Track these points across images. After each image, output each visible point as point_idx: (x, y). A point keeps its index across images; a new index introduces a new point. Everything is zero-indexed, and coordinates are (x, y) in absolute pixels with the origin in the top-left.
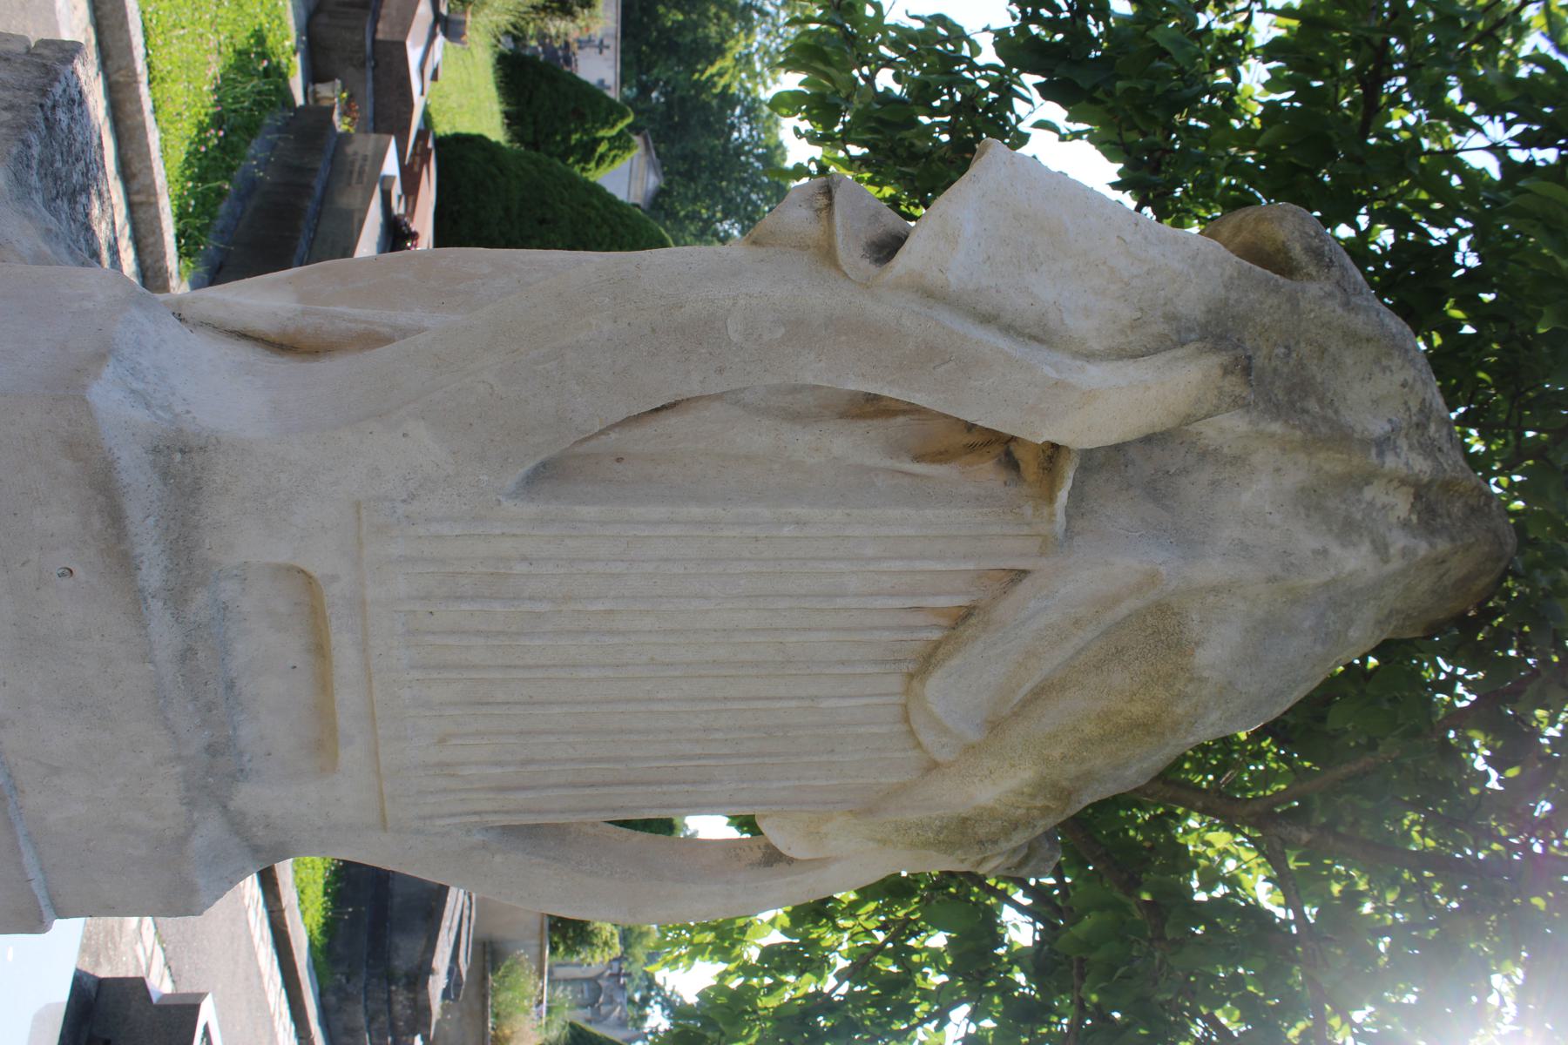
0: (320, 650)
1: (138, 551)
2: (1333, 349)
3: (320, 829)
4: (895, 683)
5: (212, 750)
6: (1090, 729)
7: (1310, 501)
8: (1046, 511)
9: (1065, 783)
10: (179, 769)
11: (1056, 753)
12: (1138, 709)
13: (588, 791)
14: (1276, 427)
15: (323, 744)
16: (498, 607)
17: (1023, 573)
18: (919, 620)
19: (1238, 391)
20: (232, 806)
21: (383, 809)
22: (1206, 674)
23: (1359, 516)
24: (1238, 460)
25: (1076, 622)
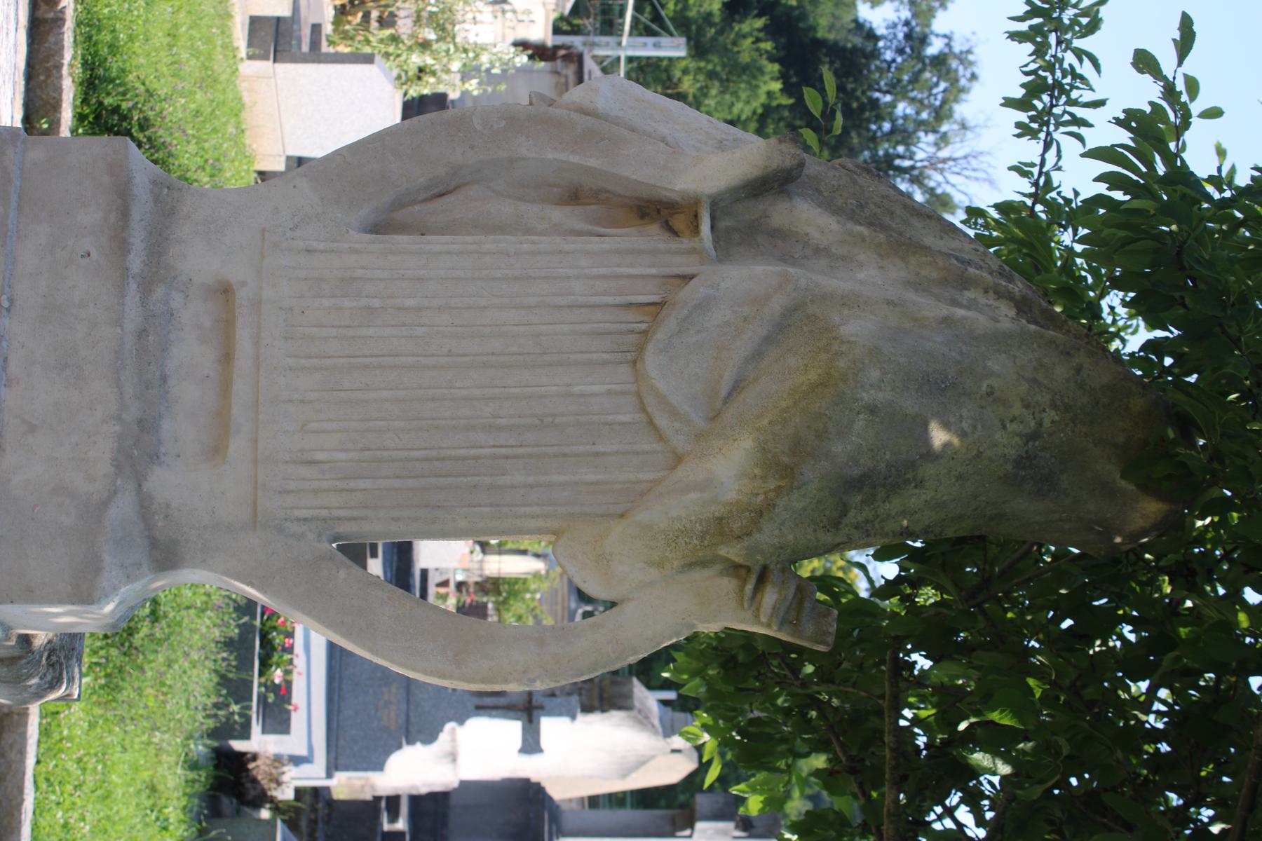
0: (227, 358)
1: (132, 240)
2: (898, 212)
3: (205, 527)
4: (624, 372)
5: (140, 422)
6: (784, 404)
7: (919, 285)
8: (696, 239)
10: (117, 428)
11: (765, 422)
12: (813, 376)
13: (411, 482)
14: (859, 228)
15: (216, 451)
16: (346, 303)
17: (692, 277)
18: (631, 316)
19: (793, 151)
20: (147, 486)
21: (255, 503)
22: (852, 339)
23: (965, 302)
24: (844, 258)
25: (745, 319)
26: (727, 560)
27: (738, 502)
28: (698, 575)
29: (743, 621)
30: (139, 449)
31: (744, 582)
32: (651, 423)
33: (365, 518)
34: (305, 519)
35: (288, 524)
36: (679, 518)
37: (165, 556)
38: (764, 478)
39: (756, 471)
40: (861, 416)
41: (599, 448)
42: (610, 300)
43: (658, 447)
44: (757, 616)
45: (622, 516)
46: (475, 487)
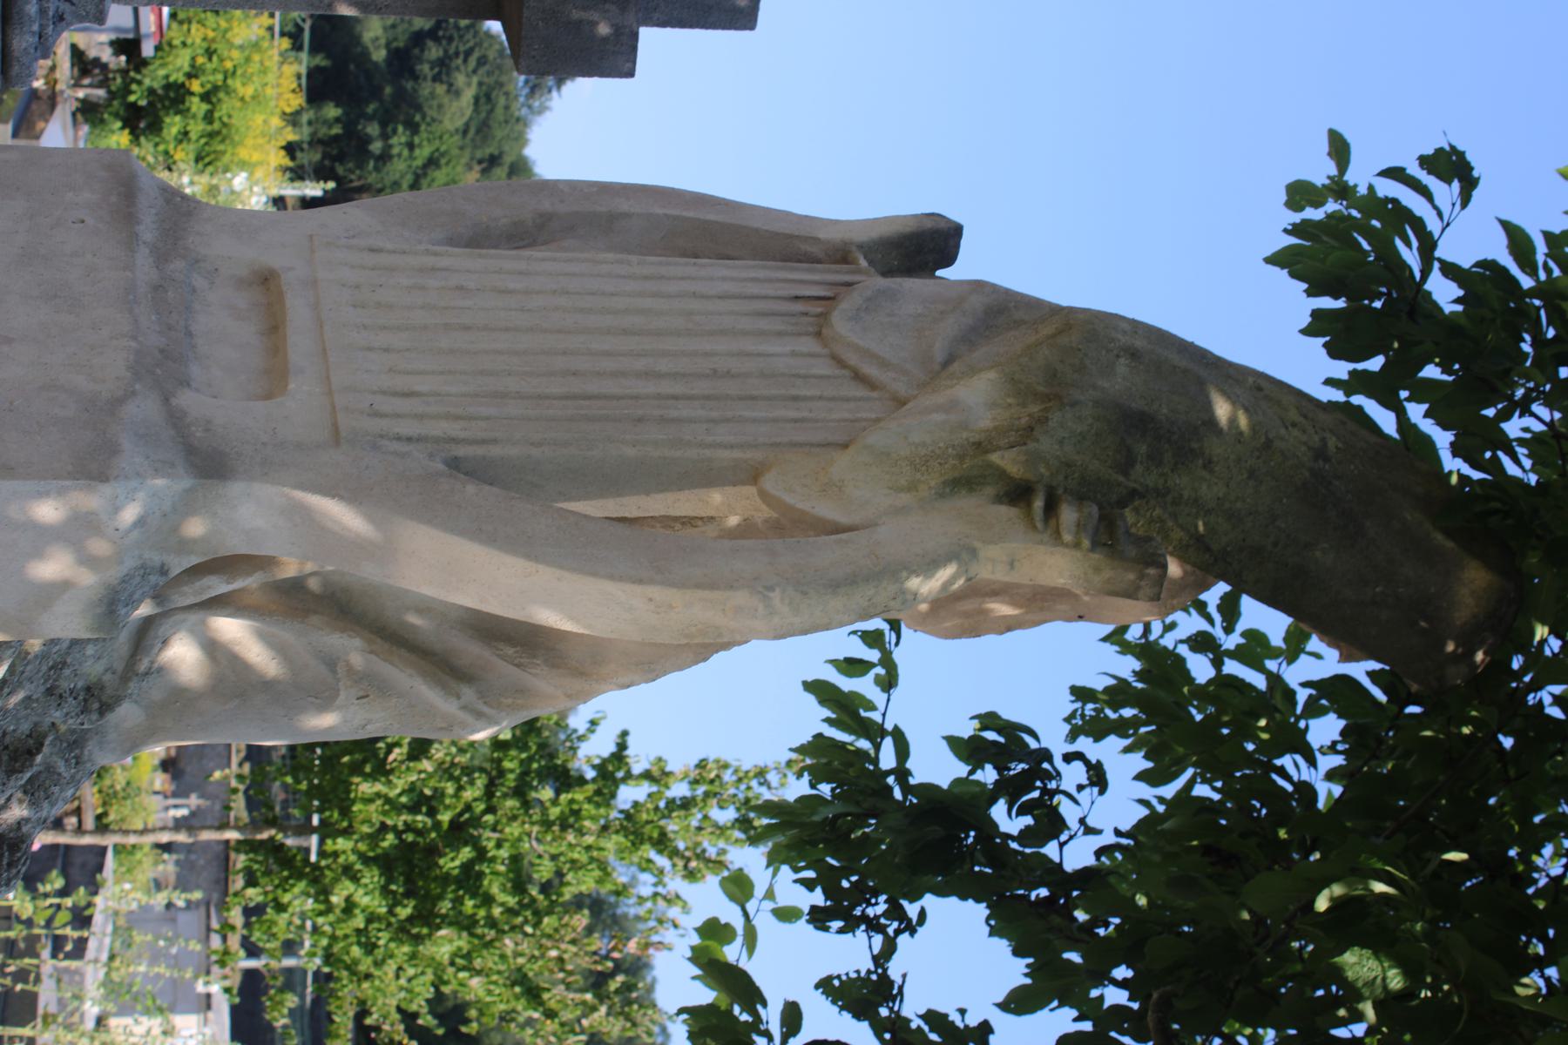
9: (1041, 389)
20: (174, 401)
26: (1002, 474)
27: (995, 428)
28: (968, 503)
29: (1041, 542)
30: (165, 367)
31: (1029, 505)
32: (858, 377)
33: (495, 441)
34: (409, 439)
35: (385, 442)
36: (924, 444)
37: (209, 463)
38: (1024, 405)
39: (1009, 400)
40: (1122, 360)
41: (794, 392)
42: (771, 292)
43: (875, 394)
44: (1057, 534)
45: (845, 446)
46: (640, 420)
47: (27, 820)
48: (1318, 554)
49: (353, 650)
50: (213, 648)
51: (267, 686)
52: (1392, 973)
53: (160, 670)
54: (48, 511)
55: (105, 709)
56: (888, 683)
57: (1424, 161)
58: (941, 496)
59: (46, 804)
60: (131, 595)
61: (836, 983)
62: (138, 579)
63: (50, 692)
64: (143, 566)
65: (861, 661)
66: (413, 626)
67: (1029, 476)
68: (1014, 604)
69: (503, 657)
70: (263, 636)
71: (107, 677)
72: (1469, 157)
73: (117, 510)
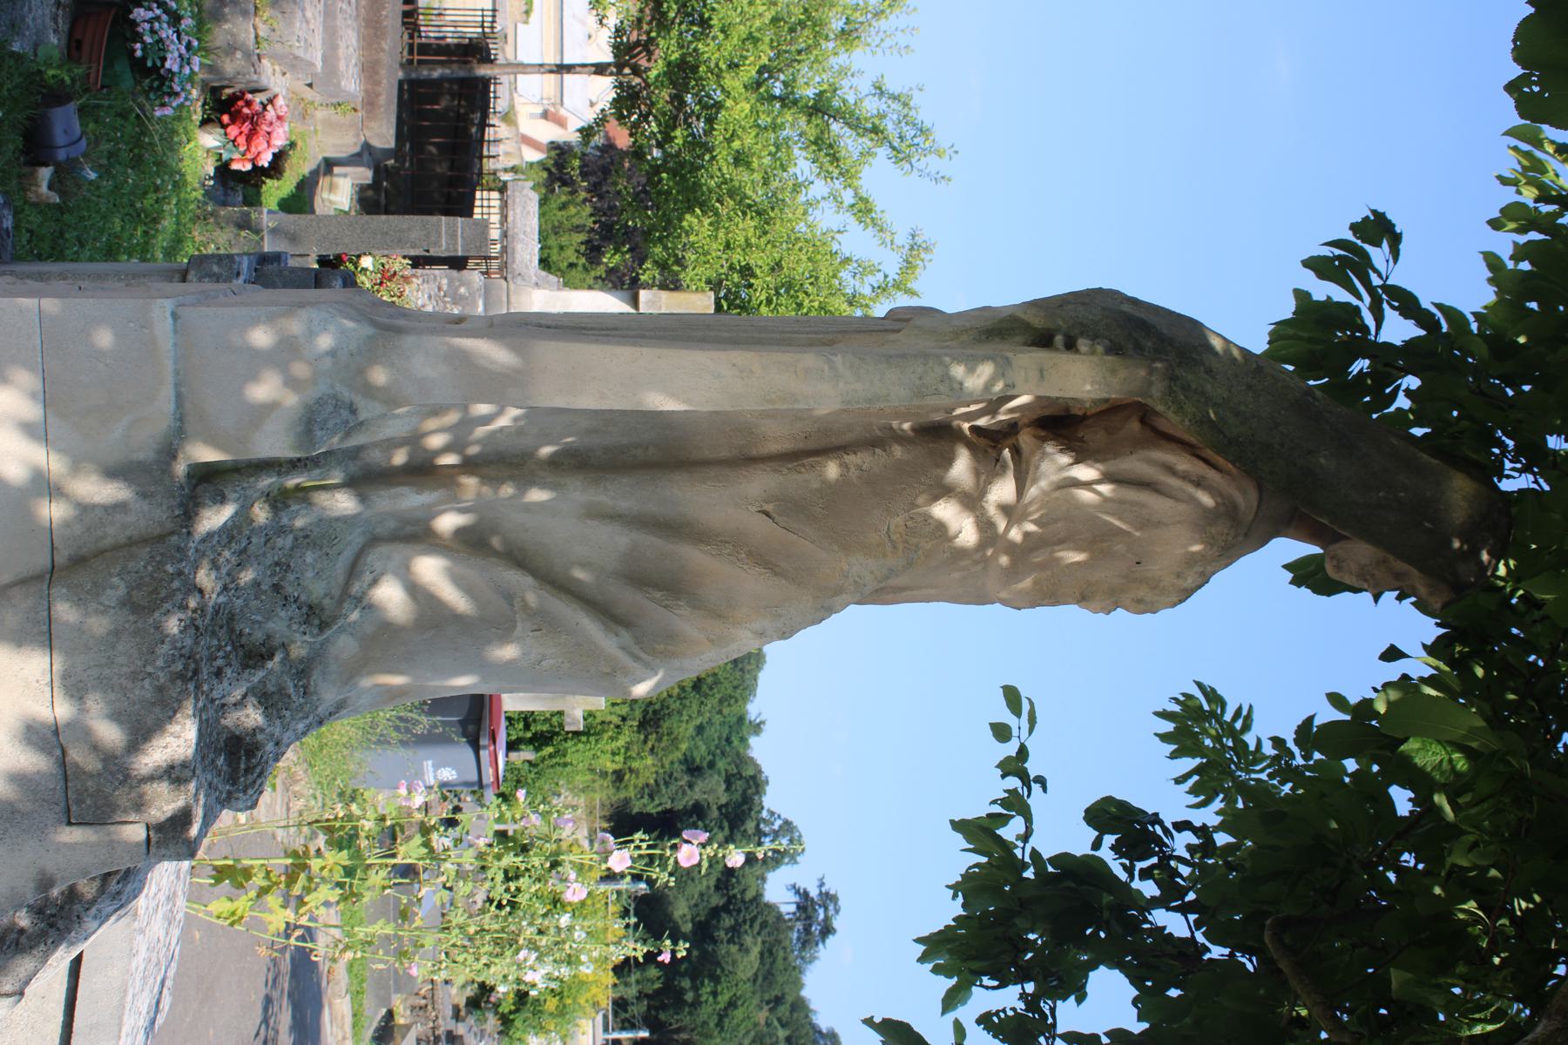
26: (1026, 327)
47: (262, 730)
48: (1322, 461)
49: (533, 595)
50: (415, 590)
51: (456, 618)
52: (1456, 756)
53: (371, 607)
54: (261, 337)
55: (323, 626)
56: (1025, 838)
57: (1354, 227)
58: (980, 341)
59: (278, 722)
60: (325, 421)
61: (995, 1019)
62: (330, 408)
63: (276, 588)
64: (334, 396)
65: (1000, 815)
66: (578, 580)
67: (1050, 325)
68: (1078, 549)
69: (653, 600)
70: (457, 580)
71: (327, 601)
72: (1389, 216)
73: (311, 334)
